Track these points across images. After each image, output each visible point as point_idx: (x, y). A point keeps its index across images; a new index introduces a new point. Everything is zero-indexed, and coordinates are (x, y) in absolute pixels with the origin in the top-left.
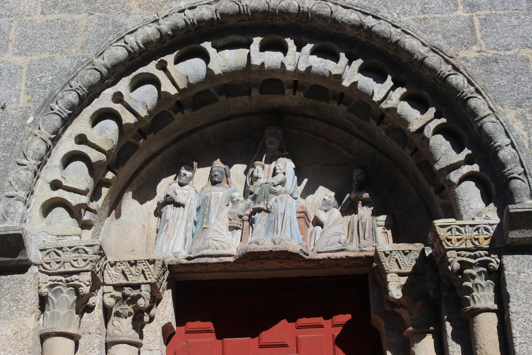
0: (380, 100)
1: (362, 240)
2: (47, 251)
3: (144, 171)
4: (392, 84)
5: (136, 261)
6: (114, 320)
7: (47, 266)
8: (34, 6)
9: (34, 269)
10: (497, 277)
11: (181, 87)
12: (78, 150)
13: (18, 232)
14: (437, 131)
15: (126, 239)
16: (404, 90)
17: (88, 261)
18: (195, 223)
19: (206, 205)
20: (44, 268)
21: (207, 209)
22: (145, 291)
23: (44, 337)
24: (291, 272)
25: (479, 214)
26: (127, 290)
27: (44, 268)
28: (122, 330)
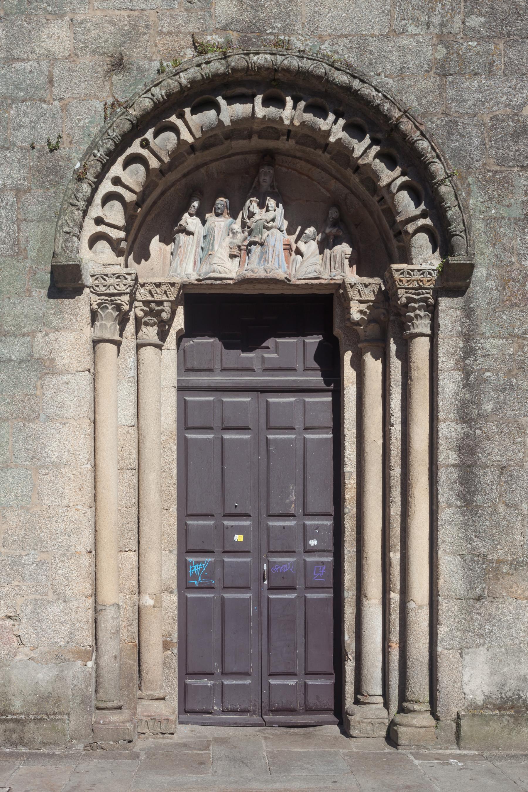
0: (358, 156)
1: (333, 270)
2: (96, 277)
3: (160, 201)
4: (370, 141)
5: (160, 283)
6: (144, 329)
7: (97, 288)
9: (87, 291)
10: (433, 311)
14: (402, 187)
16: (378, 148)
18: (202, 249)
20: (94, 290)
22: (167, 306)
23: (96, 342)
24: (276, 290)
25: (426, 261)
26: (153, 305)
27: (94, 290)
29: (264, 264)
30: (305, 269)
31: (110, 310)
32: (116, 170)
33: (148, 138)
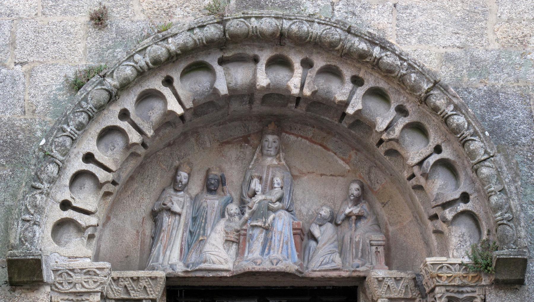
2: (60, 272)
5: (138, 278)
7: (59, 286)
8: (34, 4)
11: (187, 107)
12: (86, 169)
15: (121, 245)
17: (98, 283)
18: (191, 233)
19: (203, 216)
20: (57, 287)
21: (203, 221)
29: (269, 253)
30: (321, 259)
32: (89, 144)
33: (128, 108)
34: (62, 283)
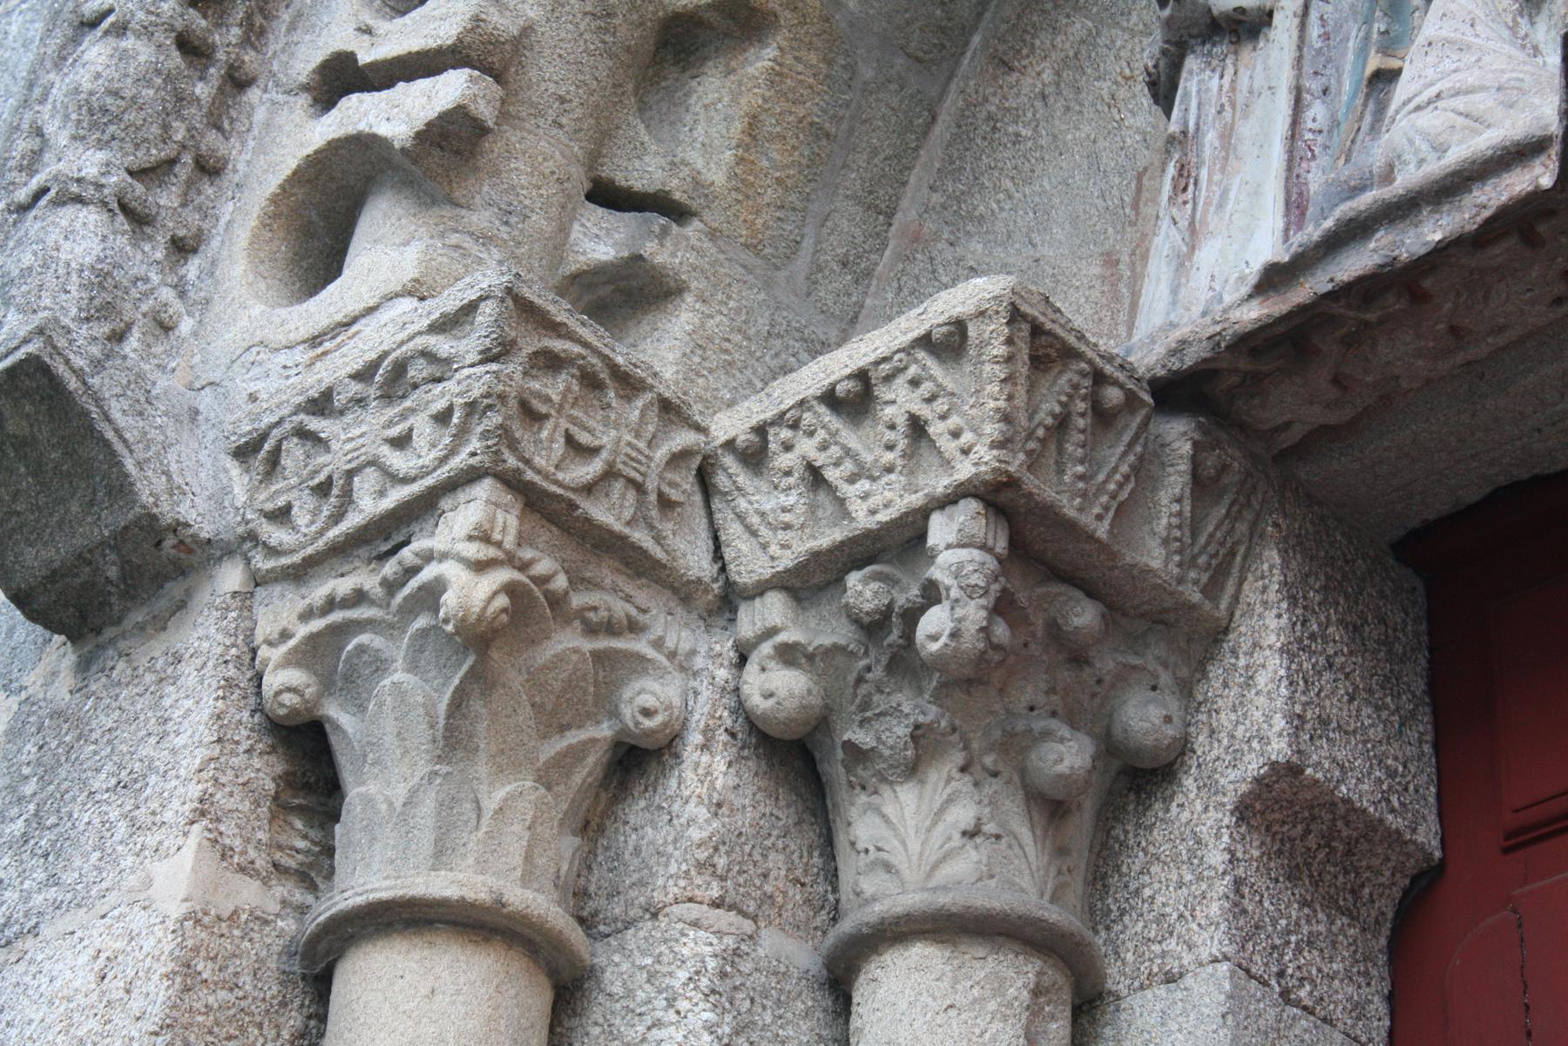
5: (862, 376)
13: (20, 355)
28: (899, 860)
31: (399, 676)
34: (287, 509)
